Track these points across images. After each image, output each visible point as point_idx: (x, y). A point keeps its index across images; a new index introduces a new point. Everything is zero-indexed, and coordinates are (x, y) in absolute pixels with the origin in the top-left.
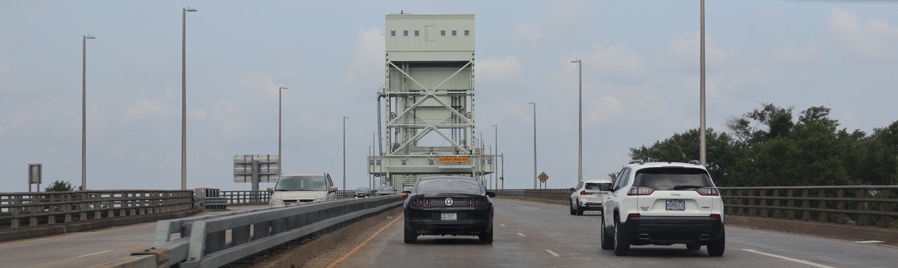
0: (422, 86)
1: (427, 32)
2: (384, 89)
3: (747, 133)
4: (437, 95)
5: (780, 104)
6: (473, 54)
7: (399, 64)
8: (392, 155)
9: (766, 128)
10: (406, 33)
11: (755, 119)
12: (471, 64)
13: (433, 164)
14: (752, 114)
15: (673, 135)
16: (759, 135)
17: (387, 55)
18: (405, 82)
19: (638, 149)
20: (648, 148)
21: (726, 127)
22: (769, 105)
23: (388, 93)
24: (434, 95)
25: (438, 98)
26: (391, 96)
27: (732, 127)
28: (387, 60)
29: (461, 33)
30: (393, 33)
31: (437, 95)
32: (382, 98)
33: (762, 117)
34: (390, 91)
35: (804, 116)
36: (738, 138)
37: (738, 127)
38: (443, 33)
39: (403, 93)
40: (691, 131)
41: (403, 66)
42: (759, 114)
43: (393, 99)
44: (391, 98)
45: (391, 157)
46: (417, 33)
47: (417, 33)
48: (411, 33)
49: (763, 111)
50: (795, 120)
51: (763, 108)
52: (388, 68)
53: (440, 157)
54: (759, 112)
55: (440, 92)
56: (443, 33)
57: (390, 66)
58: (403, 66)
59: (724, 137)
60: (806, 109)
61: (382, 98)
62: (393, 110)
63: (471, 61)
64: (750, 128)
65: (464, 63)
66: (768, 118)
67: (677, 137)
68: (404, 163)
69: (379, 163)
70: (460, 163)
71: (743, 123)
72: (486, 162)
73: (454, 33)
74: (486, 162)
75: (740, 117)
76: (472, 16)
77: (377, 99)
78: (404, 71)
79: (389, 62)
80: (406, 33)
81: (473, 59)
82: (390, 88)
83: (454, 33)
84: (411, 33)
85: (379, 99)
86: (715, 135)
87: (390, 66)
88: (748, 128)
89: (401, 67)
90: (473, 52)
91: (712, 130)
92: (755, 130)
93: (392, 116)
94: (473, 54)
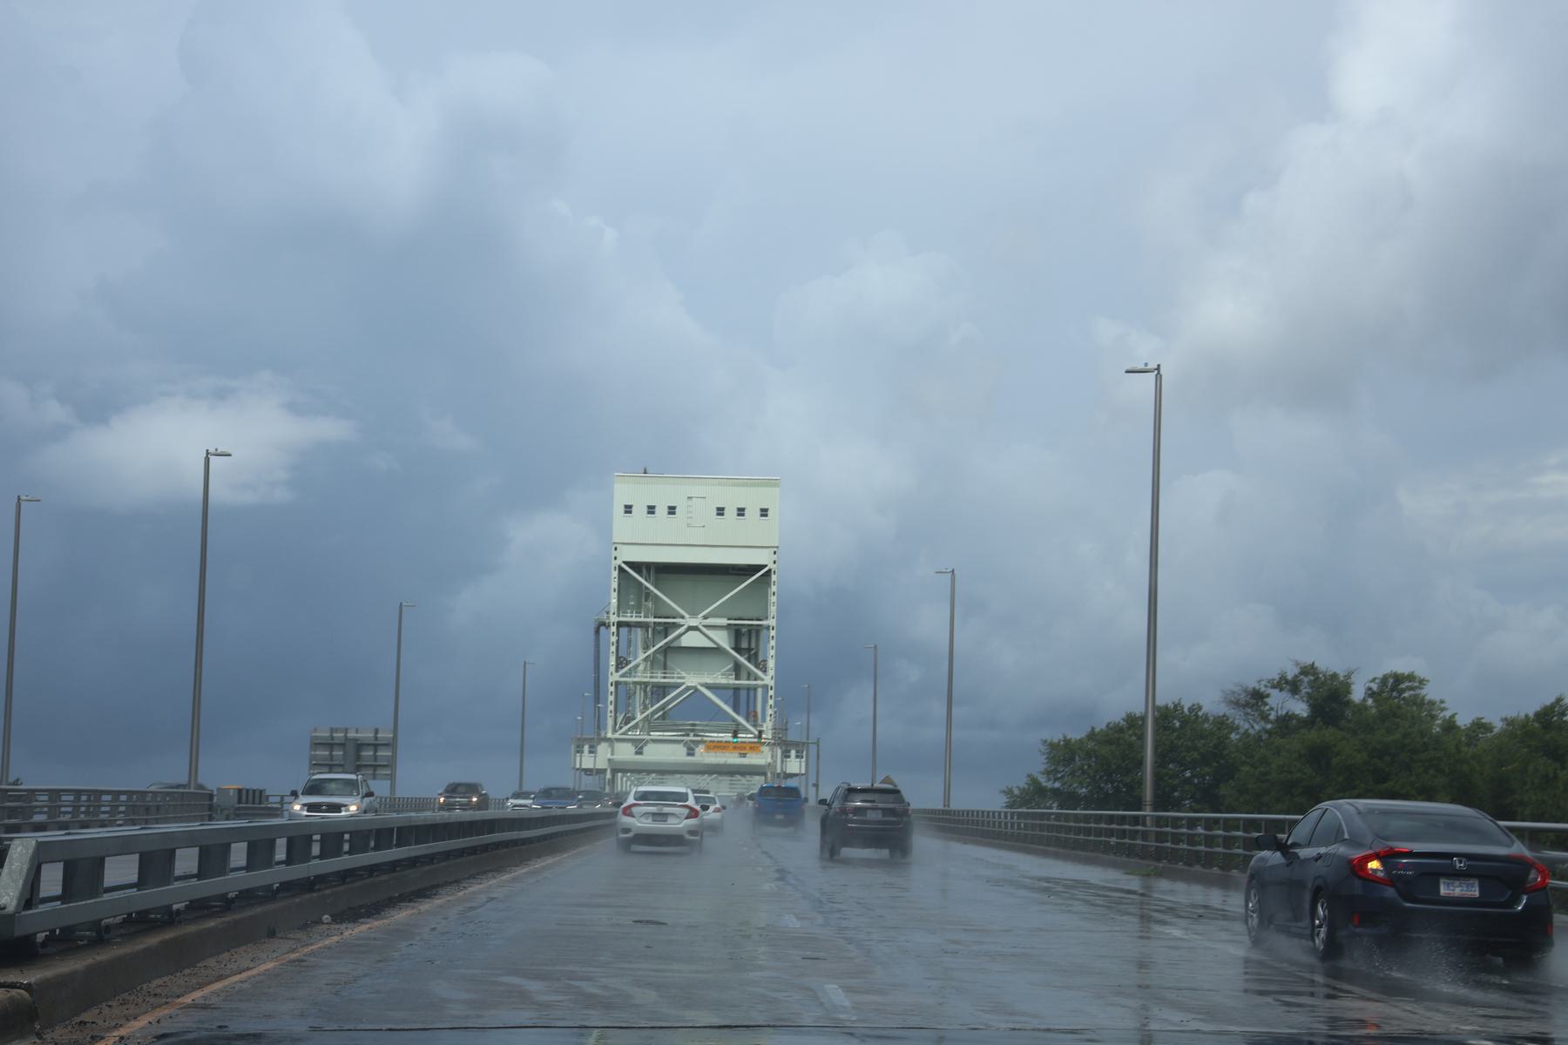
1: (690, 509)
3: (1265, 717)
4: (704, 626)
5: (1329, 662)
7: (636, 566)
8: (617, 735)
9: (1300, 708)
10: (651, 510)
11: (1281, 690)
12: (770, 570)
13: (693, 755)
14: (1275, 682)
15: (1124, 716)
16: (1287, 723)
18: (646, 601)
21: (1223, 705)
22: (1307, 664)
23: (614, 619)
24: (700, 627)
25: (704, 630)
26: (620, 625)
27: (1236, 704)
31: (704, 626)
32: (602, 628)
33: (1292, 686)
34: (619, 616)
35: (1375, 687)
36: (1247, 726)
37: (1247, 705)
38: (720, 512)
39: (642, 619)
42: (1287, 682)
43: (624, 630)
44: (621, 629)
45: (618, 740)
46: (672, 510)
47: (672, 510)
48: (662, 510)
49: (1296, 676)
50: (1357, 694)
51: (1296, 671)
52: (615, 574)
53: (706, 741)
54: (1290, 677)
56: (720, 512)
57: (619, 566)
59: (1222, 723)
60: (1380, 675)
61: (602, 628)
63: (771, 566)
64: (1272, 709)
65: (756, 568)
66: (1305, 690)
68: (639, 752)
69: (592, 751)
70: (744, 755)
71: (1258, 697)
72: (793, 753)
73: (741, 512)
74: (793, 753)
75: (1252, 684)
78: (646, 580)
79: (619, 562)
80: (651, 510)
82: (618, 610)
83: (741, 512)
84: (662, 510)
85: (597, 631)
87: (621, 570)
88: (1267, 707)
89: (639, 572)
90: (775, 549)
91: (1200, 708)
92: (1280, 713)
93: (621, 663)
94: (775, 553)
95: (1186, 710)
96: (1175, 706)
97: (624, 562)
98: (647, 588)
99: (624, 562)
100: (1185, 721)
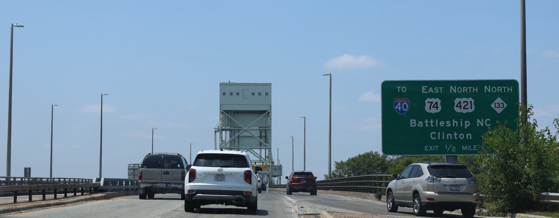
0: (239, 124)
2: (218, 126)
4: (249, 130)
6: (270, 106)
7: (227, 112)
12: (269, 112)
15: (358, 155)
17: (220, 106)
18: (230, 122)
19: (339, 162)
20: (344, 162)
24: (249, 131)
28: (220, 109)
29: (263, 94)
30: (224, 94)
31: (249, 130)
38: (253, 94)
40: (366, 153)
41: (230, 113)
43: (224, 132)
46: (238, 94)
47: (238, 94)
55: (251, 128)
58: (230, 113)
62: (224, 139)
63: (269, 110)
65: (265, 111)
67: (360, 156)
73: (260, 94)
76: (270, 85)
77: (214, 132)
78: (230, 116)
79: (222, 110)
80: (231, 94)
81: (270, 109)
84: (235, 94)
85: (216, 132)
86: (379, 155)
87: (222, 113)
91: (377, 153)
93: (223, 142)
95: (374, 153)
96: (371, 153)
97: (223, 110)
98: (230, 118)
99: (223, 110)
100: (373, 156)
